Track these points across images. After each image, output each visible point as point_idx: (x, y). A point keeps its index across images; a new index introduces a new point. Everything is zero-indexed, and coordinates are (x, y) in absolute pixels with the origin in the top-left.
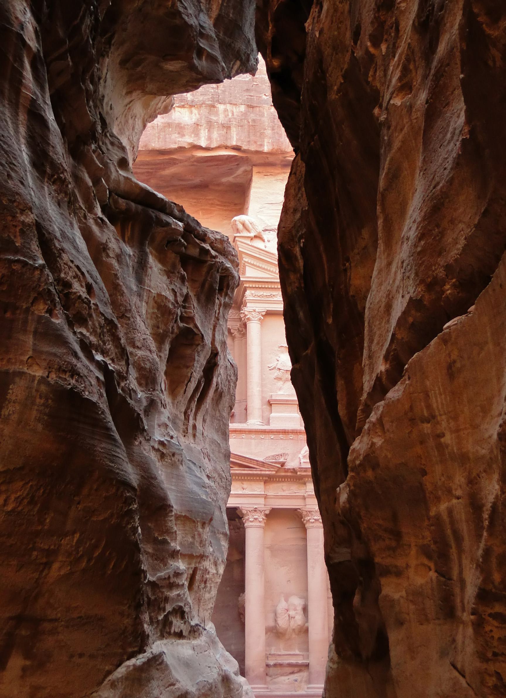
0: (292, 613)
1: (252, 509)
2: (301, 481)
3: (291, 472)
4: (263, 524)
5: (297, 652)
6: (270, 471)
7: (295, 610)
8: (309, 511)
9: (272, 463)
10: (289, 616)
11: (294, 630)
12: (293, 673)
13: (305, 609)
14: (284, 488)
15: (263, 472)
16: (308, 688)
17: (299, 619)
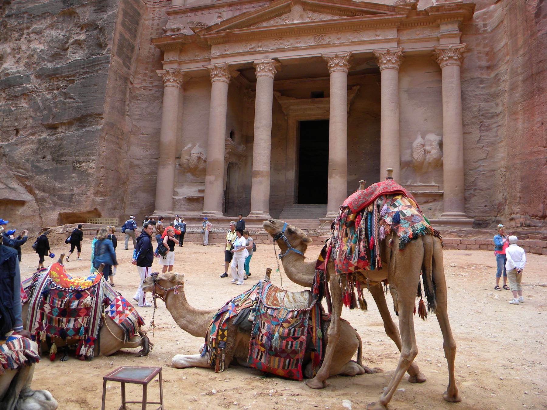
0: (428, 148)
1: (385, 52)
2: (434, 24)
3: (423, 15)
4: (396, 66)
5: (433, 184)
6: (401, 14)
7: (431, 145)
8: (443, 50)
9: (402, 5)
10: (425, 150)
11: (430, 163)
12: (427, 202)
13: (441, 145)
14: (418, 33)
15: (394, 17)
16: (442, 216)
17: (434, 153)
